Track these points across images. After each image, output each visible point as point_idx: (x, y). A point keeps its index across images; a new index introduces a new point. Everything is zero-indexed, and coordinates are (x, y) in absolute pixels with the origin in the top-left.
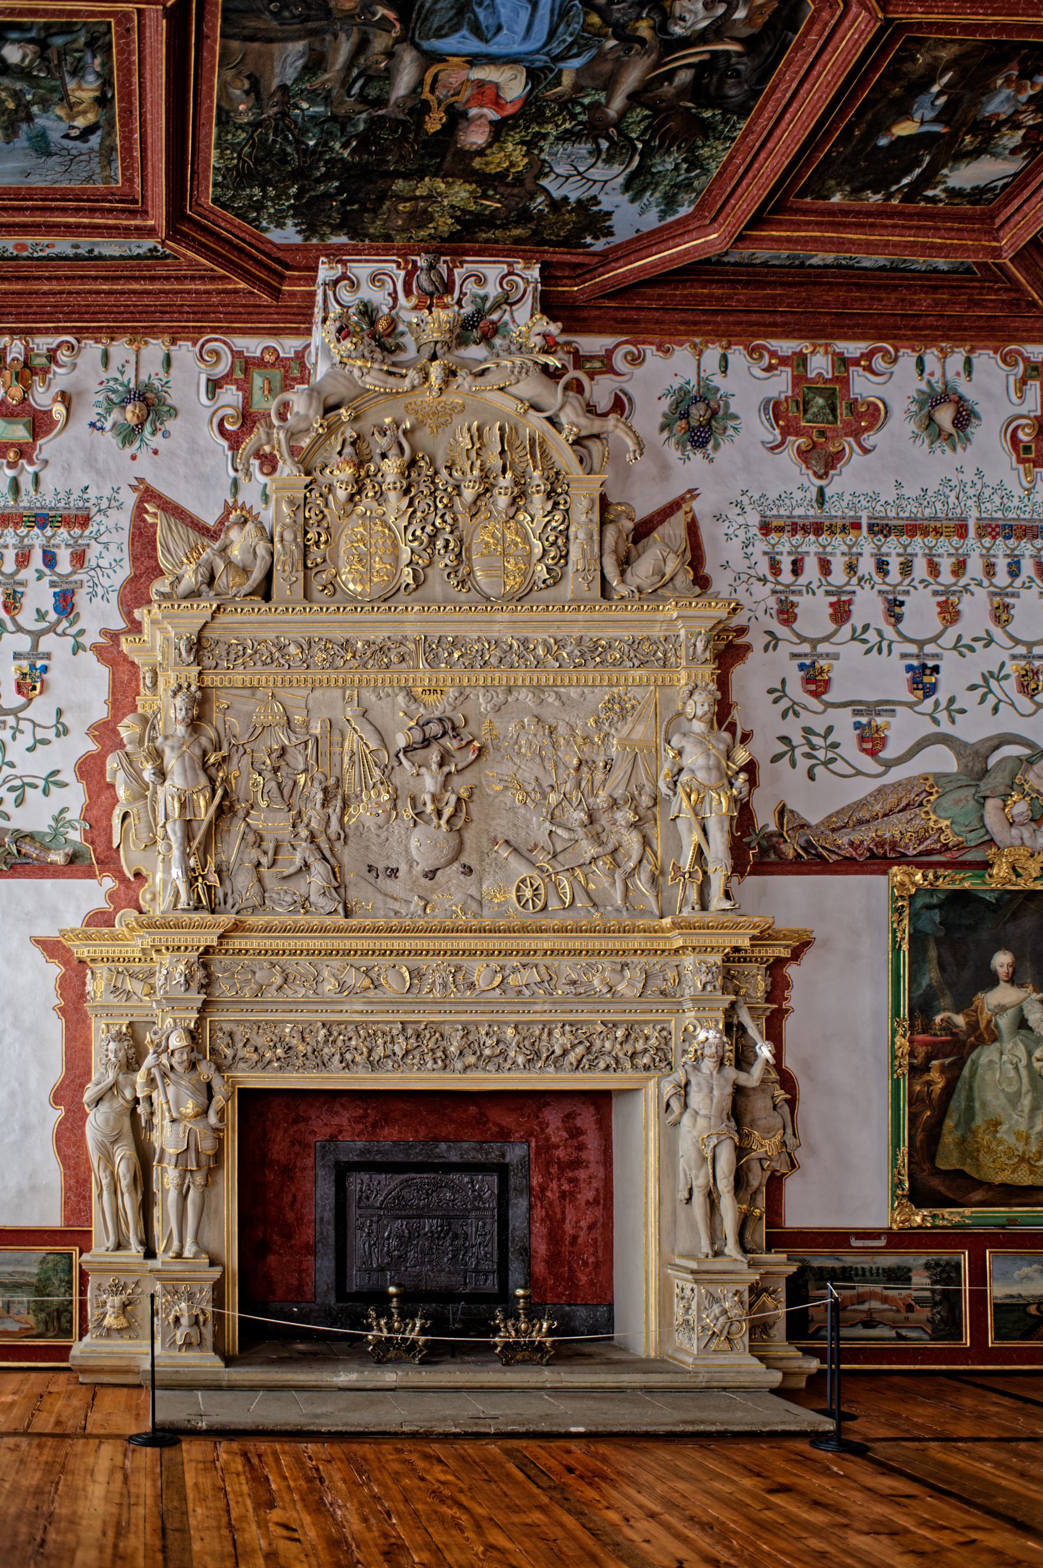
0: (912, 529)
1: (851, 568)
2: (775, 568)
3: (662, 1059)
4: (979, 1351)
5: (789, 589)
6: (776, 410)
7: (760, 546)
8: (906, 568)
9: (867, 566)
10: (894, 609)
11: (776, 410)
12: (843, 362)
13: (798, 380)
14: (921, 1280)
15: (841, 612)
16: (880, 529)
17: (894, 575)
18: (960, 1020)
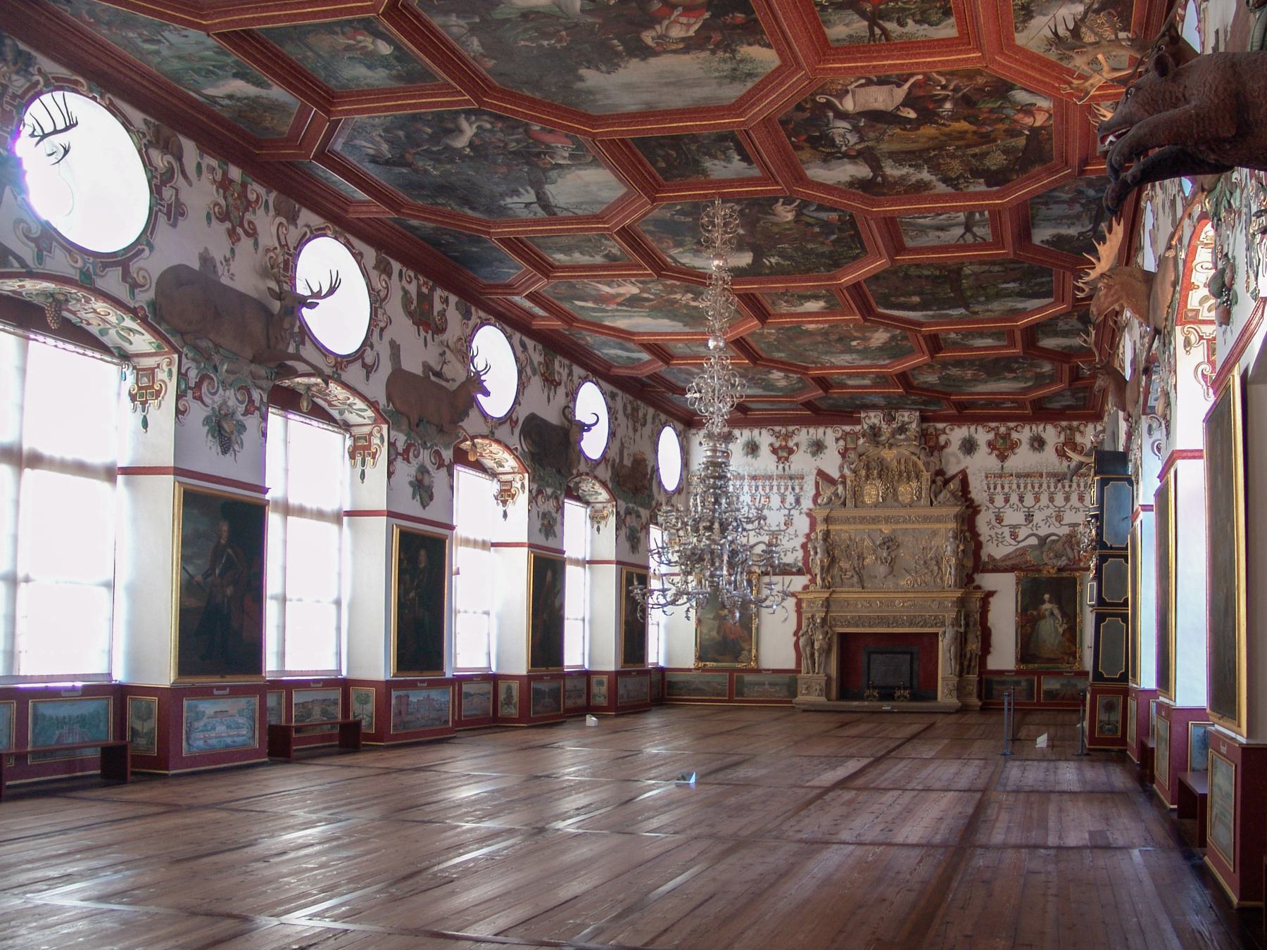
0: (1028, 475)
1: (1010, 488)
2: (989, 488)
3: (943, 624)
4: (1039, 703)
5: (993, 494)
6: (990, 444)
7: (985, 482)
8: (1025, 487)
9: (1014, 487)
10: (1021, 499)
11: (990, 444)
12: (1009, 429)
13: (996, 435)
14: (1024, 684)
15: (1007, 500)
16: (1019, 476)
17: (1022, 489)
18: (1035, 613)
